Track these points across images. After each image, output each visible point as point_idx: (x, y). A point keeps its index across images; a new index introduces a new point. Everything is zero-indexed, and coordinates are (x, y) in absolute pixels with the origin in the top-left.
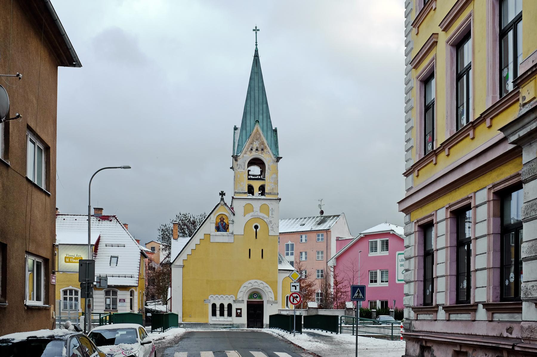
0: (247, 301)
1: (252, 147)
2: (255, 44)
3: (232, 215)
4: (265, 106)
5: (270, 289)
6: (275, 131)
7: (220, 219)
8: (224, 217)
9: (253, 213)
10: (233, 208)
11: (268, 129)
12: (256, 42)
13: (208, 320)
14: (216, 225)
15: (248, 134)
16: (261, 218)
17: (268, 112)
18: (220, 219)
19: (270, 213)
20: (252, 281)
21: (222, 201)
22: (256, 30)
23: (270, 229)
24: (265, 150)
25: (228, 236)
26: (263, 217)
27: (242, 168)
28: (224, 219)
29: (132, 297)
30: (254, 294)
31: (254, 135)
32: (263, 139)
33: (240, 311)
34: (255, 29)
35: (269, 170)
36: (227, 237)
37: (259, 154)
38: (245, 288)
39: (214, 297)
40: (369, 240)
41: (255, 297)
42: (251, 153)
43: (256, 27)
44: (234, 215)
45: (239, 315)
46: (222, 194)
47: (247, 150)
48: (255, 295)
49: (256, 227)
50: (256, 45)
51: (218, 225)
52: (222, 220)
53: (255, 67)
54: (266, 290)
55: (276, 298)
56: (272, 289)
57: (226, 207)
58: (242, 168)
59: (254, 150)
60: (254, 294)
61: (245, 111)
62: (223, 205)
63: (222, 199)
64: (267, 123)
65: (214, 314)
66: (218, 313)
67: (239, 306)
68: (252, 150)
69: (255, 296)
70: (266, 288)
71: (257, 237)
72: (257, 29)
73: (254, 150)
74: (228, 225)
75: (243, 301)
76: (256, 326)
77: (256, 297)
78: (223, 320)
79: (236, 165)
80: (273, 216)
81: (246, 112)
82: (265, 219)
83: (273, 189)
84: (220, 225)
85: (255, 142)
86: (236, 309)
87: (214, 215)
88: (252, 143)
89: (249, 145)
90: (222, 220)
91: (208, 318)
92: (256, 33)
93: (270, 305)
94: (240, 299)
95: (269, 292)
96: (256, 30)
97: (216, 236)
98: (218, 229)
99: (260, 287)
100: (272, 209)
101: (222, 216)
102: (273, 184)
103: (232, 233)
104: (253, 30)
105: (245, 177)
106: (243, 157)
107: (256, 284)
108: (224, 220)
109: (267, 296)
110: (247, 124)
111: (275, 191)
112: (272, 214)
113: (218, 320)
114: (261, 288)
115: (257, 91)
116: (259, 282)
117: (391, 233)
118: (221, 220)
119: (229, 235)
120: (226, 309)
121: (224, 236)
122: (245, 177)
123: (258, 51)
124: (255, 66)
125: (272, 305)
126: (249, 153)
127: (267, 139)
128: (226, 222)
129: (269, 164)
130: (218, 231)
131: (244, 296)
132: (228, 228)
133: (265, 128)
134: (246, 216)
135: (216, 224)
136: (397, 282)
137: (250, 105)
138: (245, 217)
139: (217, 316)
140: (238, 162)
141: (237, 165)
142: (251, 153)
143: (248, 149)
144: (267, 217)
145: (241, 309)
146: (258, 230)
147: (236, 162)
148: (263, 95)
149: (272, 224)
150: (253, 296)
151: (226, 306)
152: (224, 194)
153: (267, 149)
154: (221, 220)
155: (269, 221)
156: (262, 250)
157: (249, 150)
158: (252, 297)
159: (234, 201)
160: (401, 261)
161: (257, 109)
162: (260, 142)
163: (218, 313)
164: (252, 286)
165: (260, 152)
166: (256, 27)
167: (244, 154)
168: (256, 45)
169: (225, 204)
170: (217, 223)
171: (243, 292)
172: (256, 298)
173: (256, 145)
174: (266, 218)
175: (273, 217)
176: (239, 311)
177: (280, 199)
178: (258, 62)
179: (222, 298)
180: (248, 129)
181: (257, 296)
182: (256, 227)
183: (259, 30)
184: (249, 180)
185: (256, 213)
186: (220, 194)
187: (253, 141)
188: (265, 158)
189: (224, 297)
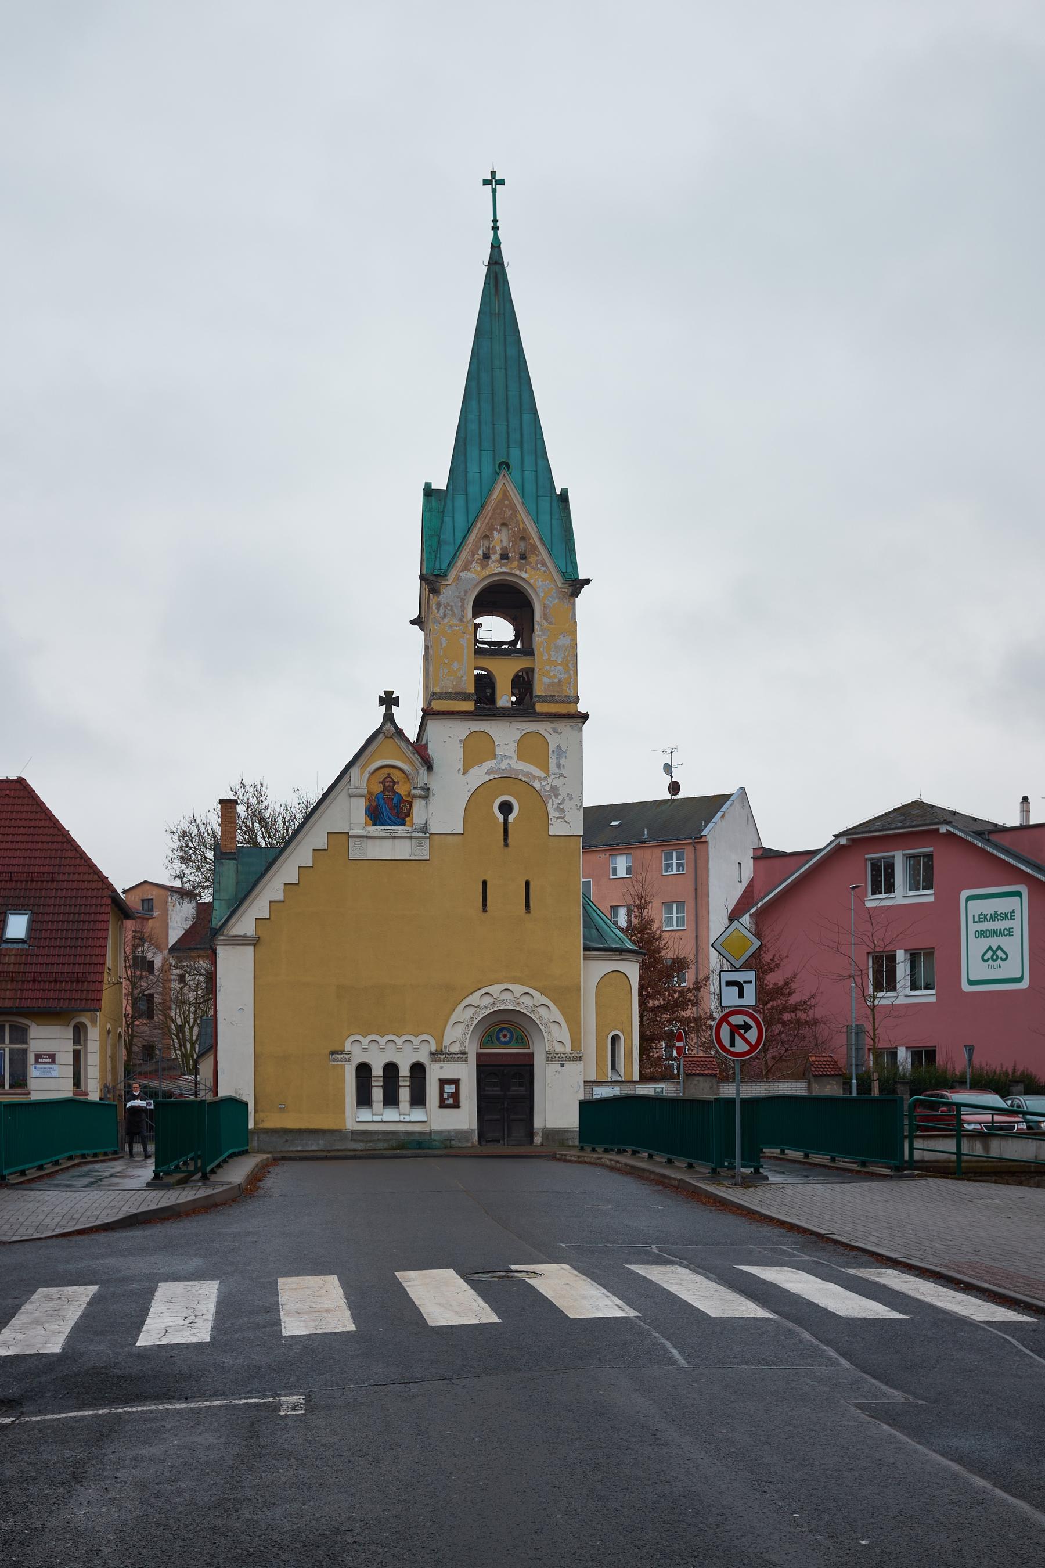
1: (488, 548)
2: (492, 224)
3: (423, 771)
4: (527, 417)
5: (556, 1014)
6: (564, 497)
7: (382, 782)
8: (396, 775)
9: (495, 761)
10: (425, 747)
12: (495, 221)
13: (344, 1120)
14: (368, 804)
15: (474, 506)
16: (520, 776)
17: (538, 437)
18: (382, 782)
19: (553, 761)
20: (495, 989)
21: (388, 726)
22: (493, 182)
23: (552, 813)
24: (533, 559)
25: (410, 838)
26: (529, 774)
28: (395, 783)
29: (79, 1047)
30: (501, 1030)
31: (494, 510)
32: (523, 521)
33: (453, 1086)
34: (490, 178)
35: (545, 624)
36: (407, 841)
37: (514, 568)
38: (472, 1010)
39: (365, 1041)
40: (867, 856)
41: (503, 1039)
42: (484, 567)
43: (493, 173)
44: (430, 768)
45: (451, 1101)
46: (389, 700)
47: (470, 558)
48: (505, 1032)
49: (506, 808)
50: (495, 228)
51: (374, 804)
52: (389, 785)
53: (493, 298)
55: (576, 1041)
56: (564, 1014)
57: (403, 744)
59: (495, 557)
60: (501, 1030)
63: (389, 717)
65: (364, 1099)
66: (377, 1094)
67: (449, 1070)
68: (486, 556)
69: (505, 1036)
70: (542, 1011)
71: (510, 841)
72: (497, 178)
73: (495, 557)
74: (411, 803)
75: (465, 1053)
76: (508, 1137)
77: (507, 1039)
78: (397, 1119)
79: (434, 607)
80: (562, 771)
82: (537, 781)
83: (560, 681)
84: (381, 802)
85: (499, 532)
86: (440, 1080)
87: (363, 768)
88: (486, 537)
89: (479, 542)
90: (389, 785)
91: (343, 1112)
92: (494, 191)
93: (556, 1066)
94: (455, 1049)
95: (550, 1024)
96: (493, 182)
97: (370, 842)
98: (375, 815)
99: (523, 1006)
100: (559, 747)
101: (389, 774)
102: (560, 667)
103: (425, 829)
104: (484, 180)
105: (465, 645)
107: (507, 996)
108: (394, 785)
109: (546, 1035)
110: (470, 475)
111: (568, 691)
112: (559, 766)
113: (377, 1118)
114: (525, 1011)
115: (499, 374)
116: (518, 989)
117: (941, 832)
118: (384, 786)
119: (414, 834)
120: (406, 1081)
121: (397, 841)
122: (465, 645)
123: (499, 247)
124: (493, 291)
125: (562, 1065)
126: (479, 569)
127: (537, 522)
128: (403, 793)
130: (375, 825)
131: (468, 1036)
132: (409, 813)
133: (530, 487)
134: (471, 771)
135: (370, 800)
136: (966, 987)
137: (480, 415)
138: (467, 775)
139: (375, 1105)
140: (441, 596)
141: (439, 605)
142: (484, 567)
143: (473, 555)
144: (544, 775)
145: (456, 1082)
146: (511, 818)
147: (436, 598)
148: (520, 383)
149: (560, 798)
150: (498, 1039)
151: (404, 1071)
152: (396, 702)
153: (537, 555)
154: (387, 784)
155: (548, 788)
156: (527, 884)
158: (494, 1039)
159: (432, 726)
160: (977, 919)
161: (501, 428)
163: (377, 1094)
164: (494, 1004)
165: (516, 563)
166: (493, 173)
167: (463, 571)
168: (495, 228)
169: (400, 732)
170: (370, 797)
171: (461, 1026)
172: (505, 1043)
173: (501, 539)
174: (540, 779)
175: (562, 775)
176: (450, 1089)
177: (585, 717)
178: (501, 280)
179: (391, 1045)
180: (474, 490)
181: (511, 1038)
182: (506, 808)
183: (502, 182)
184: (478, 656)
185: (508, 761)
186: (382, 701)
187: (492, 529)
188: (532, 581)
189: (399, 1041)
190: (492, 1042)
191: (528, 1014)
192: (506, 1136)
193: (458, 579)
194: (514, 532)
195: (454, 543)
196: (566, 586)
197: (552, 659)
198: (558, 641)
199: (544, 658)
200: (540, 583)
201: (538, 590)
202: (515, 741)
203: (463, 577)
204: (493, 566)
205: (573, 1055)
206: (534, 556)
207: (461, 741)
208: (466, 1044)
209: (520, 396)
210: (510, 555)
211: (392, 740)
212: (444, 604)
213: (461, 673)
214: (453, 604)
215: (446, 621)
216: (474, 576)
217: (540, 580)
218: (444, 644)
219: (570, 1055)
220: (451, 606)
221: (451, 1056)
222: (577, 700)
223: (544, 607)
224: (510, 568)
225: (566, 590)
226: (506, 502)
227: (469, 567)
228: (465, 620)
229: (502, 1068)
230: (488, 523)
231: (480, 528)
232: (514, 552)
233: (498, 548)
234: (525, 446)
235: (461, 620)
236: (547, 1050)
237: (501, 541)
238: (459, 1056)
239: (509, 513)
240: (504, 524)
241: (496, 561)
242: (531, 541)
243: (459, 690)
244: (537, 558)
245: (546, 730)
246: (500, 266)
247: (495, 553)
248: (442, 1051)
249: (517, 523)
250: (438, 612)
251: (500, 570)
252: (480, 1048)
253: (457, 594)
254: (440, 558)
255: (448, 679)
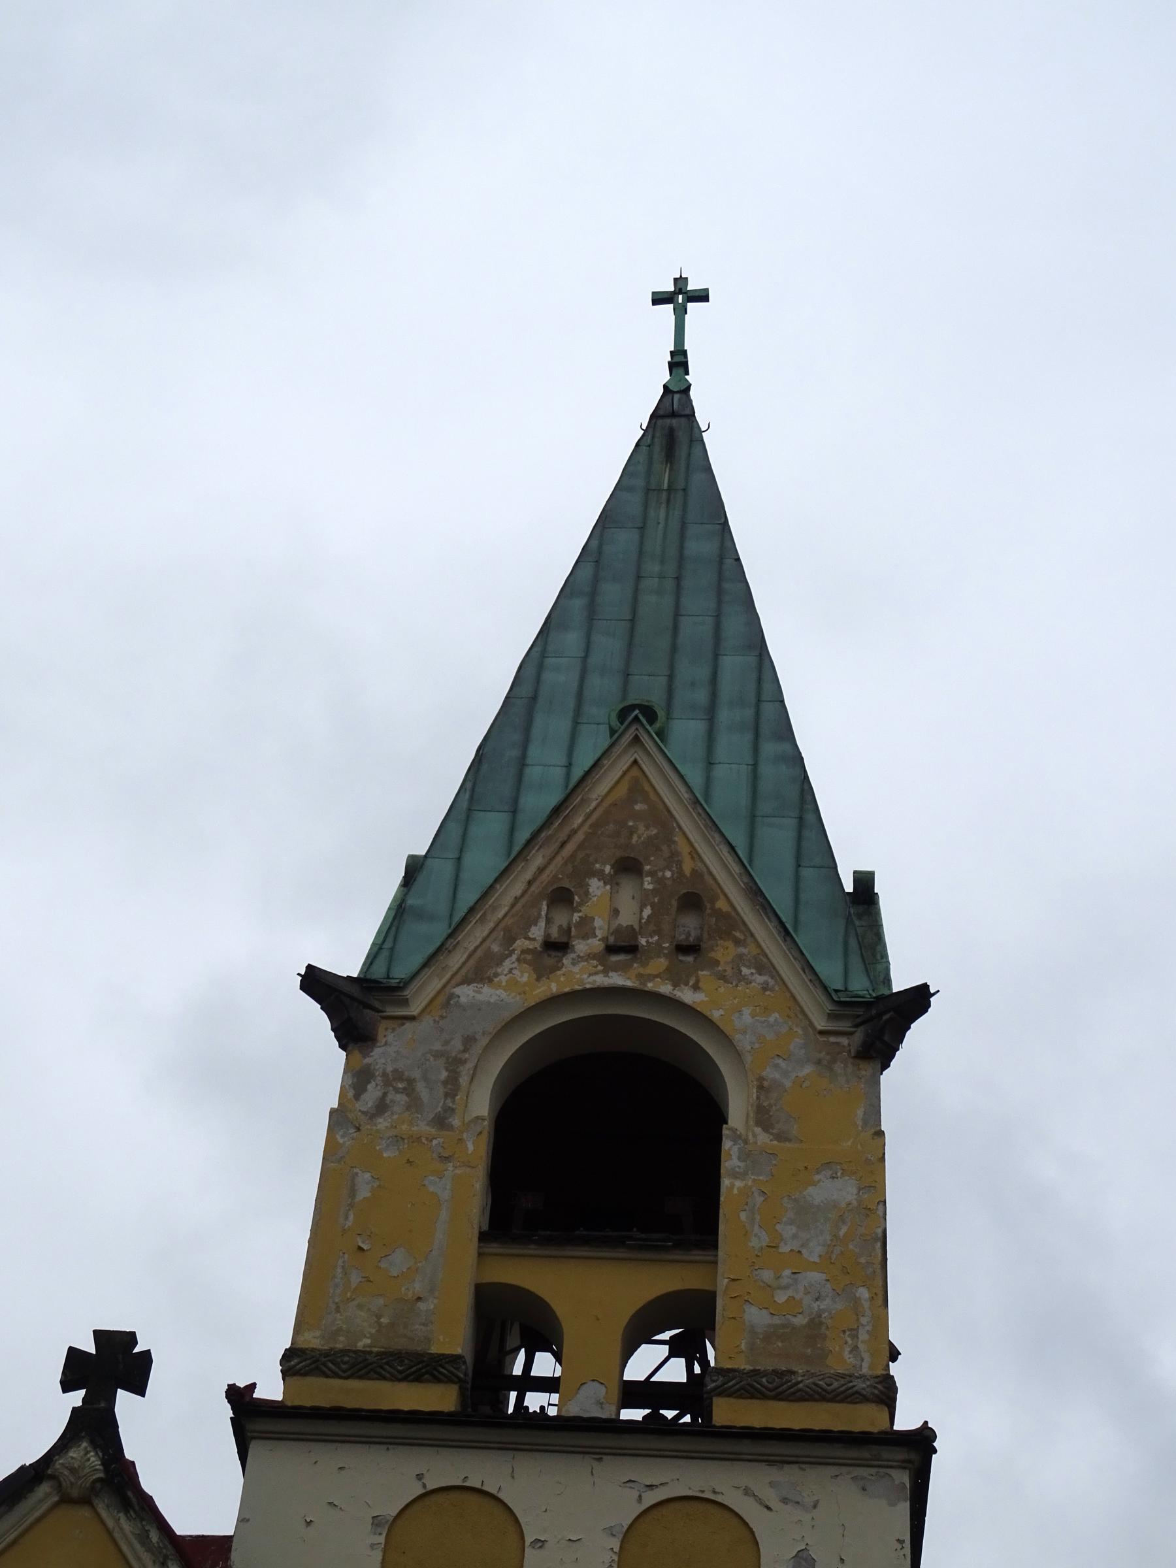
4: (733, 664)
11: (764, 807)
24: (724, 952)
27: (414, 1104)
32: (695, 854)
37: (652, 977)
42: (542, 973)
47: (496, 948)
57: (126, 1526)
58: (414, 1104)
61: (526, 690)
62: (85, 1501)
64: (755, 765)
81: (534, 698)
83: (816, 1323)
85: (612, 881)
102: (815, 1277)
106: (447, 1005)
126: (524, 976)
129: (771, 1074)
140: (377, 1051)
142: (542, 973)
143: (510, 939)
153: (738, 942)
157: (521, 944)
162: (660, 881)
167: (466, 981)
178: (682, 437)
183: (702, 296)
184: (494, 1248)
187: (583, 872)
188: (716, 1015)
193: (447, 1005)
194: (660, 881)
195: (451, 915)
196: (844, 1026)
197: (785, 1249)
198: (811, 1189)
199: (754, 1243)
200: (747, 1017)
201: (737, 1037)
202: (610, 1532)
203: (463, 1000)
204: (576, 969)
206: (729, 944)
207: (377, 1521)
209: (718, 626)
210: (643, 941)
211: (84, 1512)
212: (384, 1074)
213: (418, 1287)
214: (416, 1074)
215: (382, 1123)
216: (502, 993)
217: (747, 1012)
218: (363, 1193)
220: (411, 1082)
222: (886, 1394)
223: (761, 1088)
224: (640, 976)
225: (844, 1041)
226: (638, 807)
227: (491, 972)
228: (456, 1122)
230: (573, 856)
231: (541, 870)
232: (658, 932)
233: (598, 922)
234: (724, 715)
235: (441, 1122)
237: (616, 912)
239: (644, 832)
240: (628, 867)
241: (590, 956)
242: (721, 904)
243: (400, 1344)
244: (742, 950)
245: (747, 1492)
246: (683, 420)
247: (589, 934)
249: (674, 859)
250: (357, 1097)
251: (600, 980)
253: (438, 1046)
254: (392, 949)
255: (360, 1307)
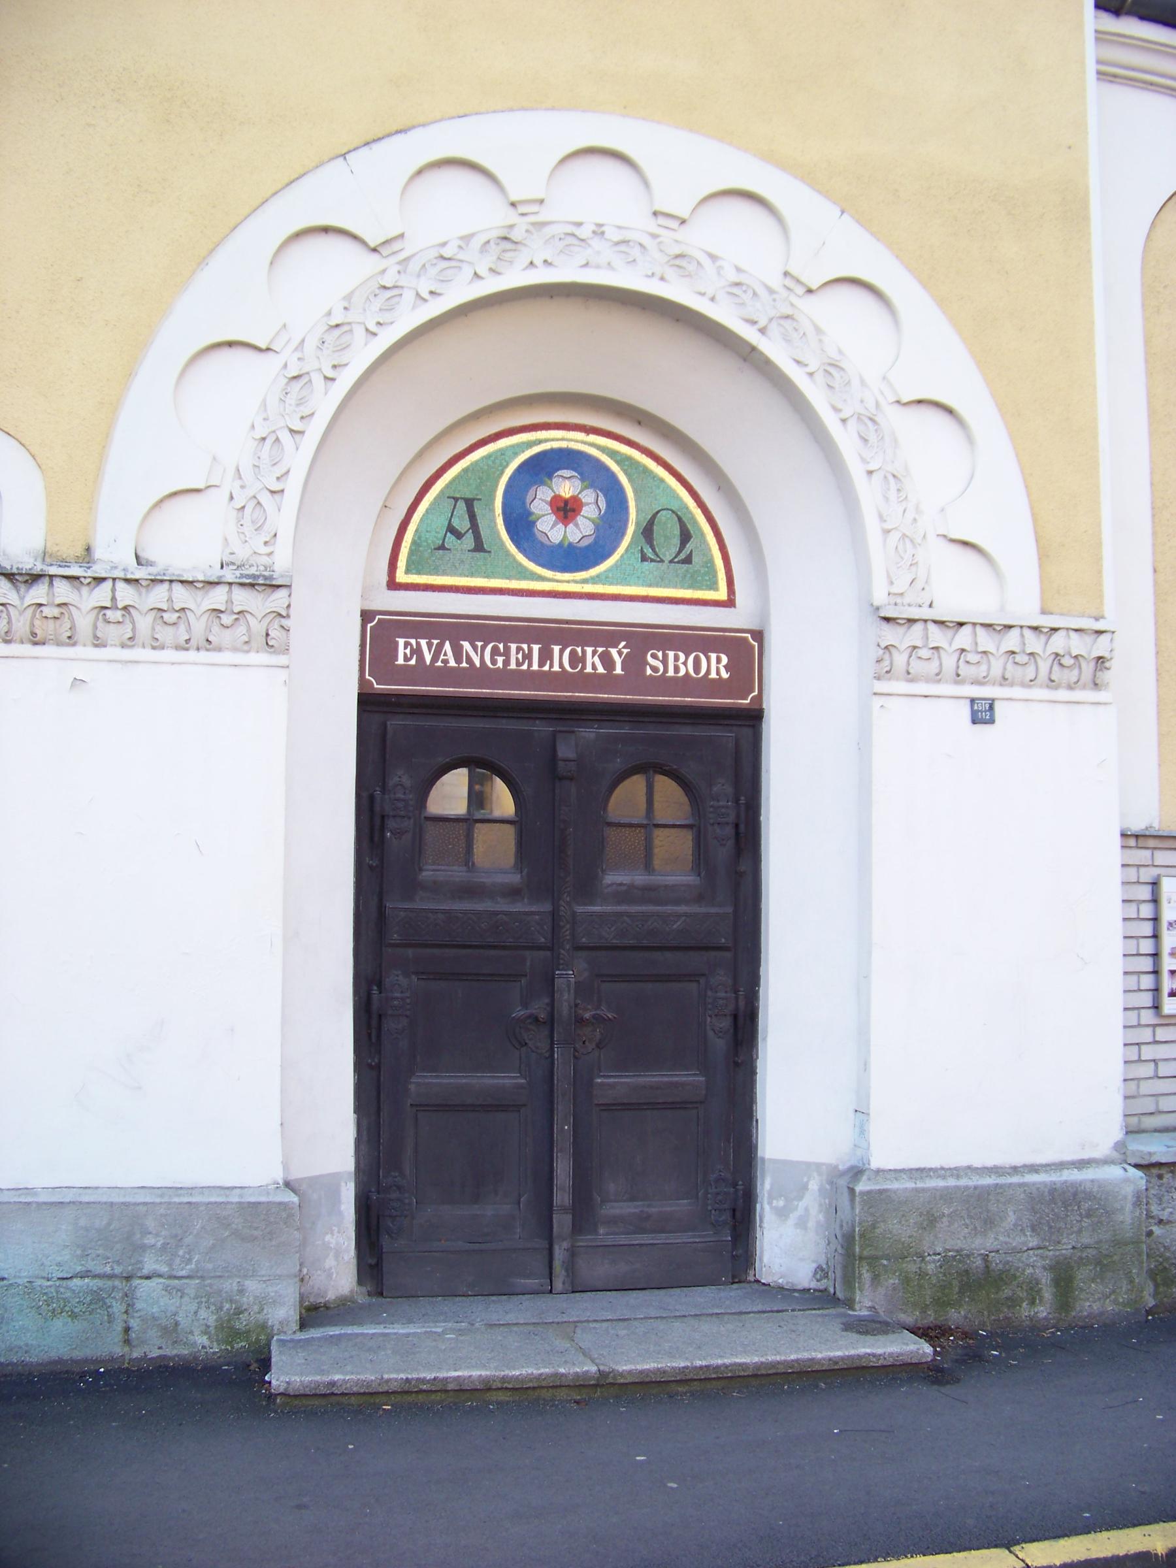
0: (366, 616)
48: (566, 486)
54: (833, 366)
69: (566, 510)
77: (580, 531)
95: (898, 421)
131: (299, 458)
190: (479, 547)
191: (749, 334)
192: (562, 1222)
205: (1058, 643)
208: (284, 517)
219: (1034, 643)
221: (159, 595)
229: (542, 728)
236: (880, 596)
238: (218, 598)
248: (88, 555)
252: (393, 585)
